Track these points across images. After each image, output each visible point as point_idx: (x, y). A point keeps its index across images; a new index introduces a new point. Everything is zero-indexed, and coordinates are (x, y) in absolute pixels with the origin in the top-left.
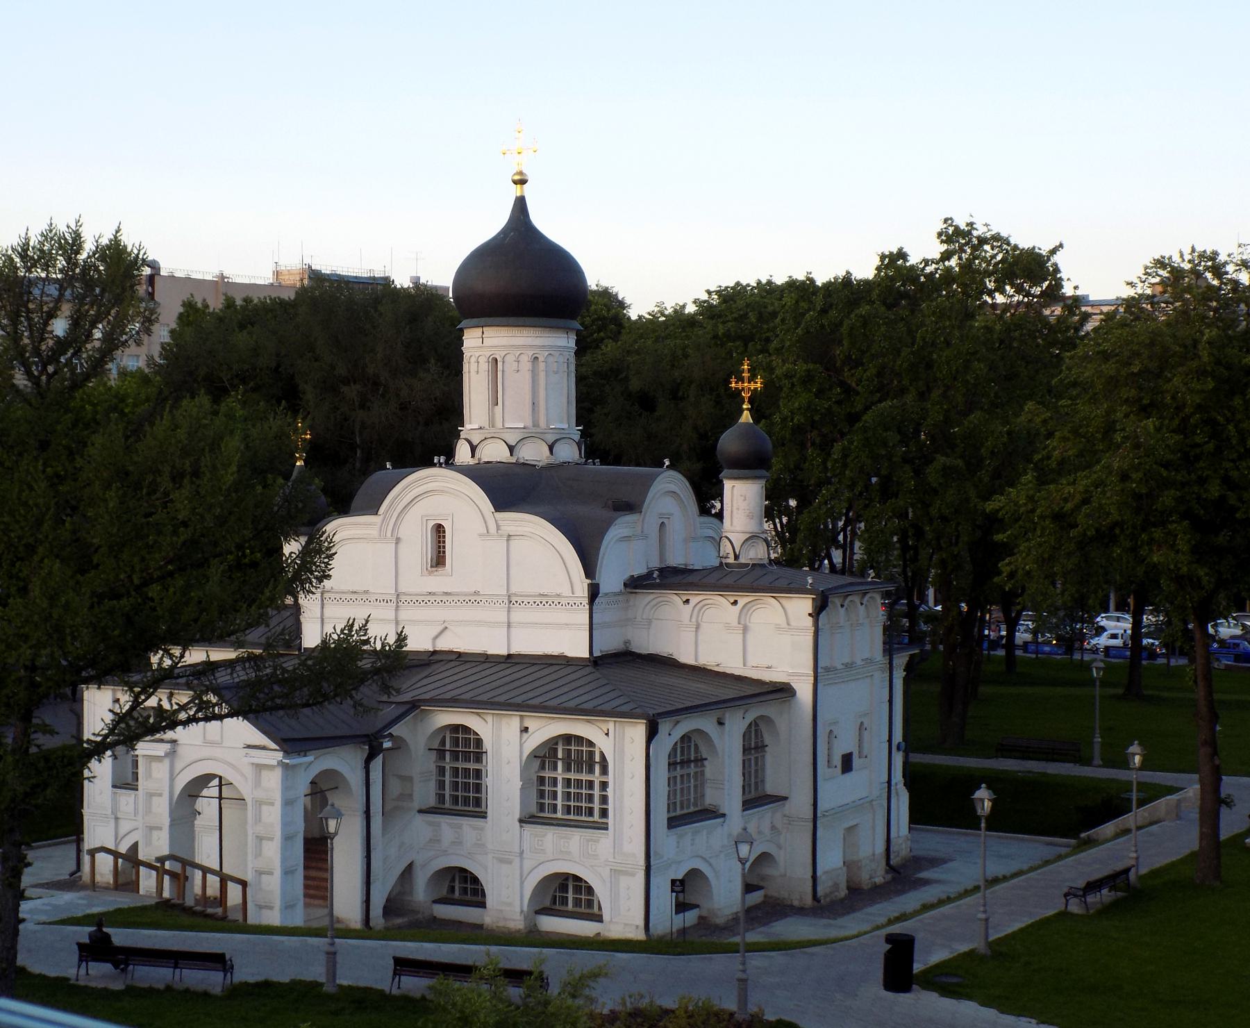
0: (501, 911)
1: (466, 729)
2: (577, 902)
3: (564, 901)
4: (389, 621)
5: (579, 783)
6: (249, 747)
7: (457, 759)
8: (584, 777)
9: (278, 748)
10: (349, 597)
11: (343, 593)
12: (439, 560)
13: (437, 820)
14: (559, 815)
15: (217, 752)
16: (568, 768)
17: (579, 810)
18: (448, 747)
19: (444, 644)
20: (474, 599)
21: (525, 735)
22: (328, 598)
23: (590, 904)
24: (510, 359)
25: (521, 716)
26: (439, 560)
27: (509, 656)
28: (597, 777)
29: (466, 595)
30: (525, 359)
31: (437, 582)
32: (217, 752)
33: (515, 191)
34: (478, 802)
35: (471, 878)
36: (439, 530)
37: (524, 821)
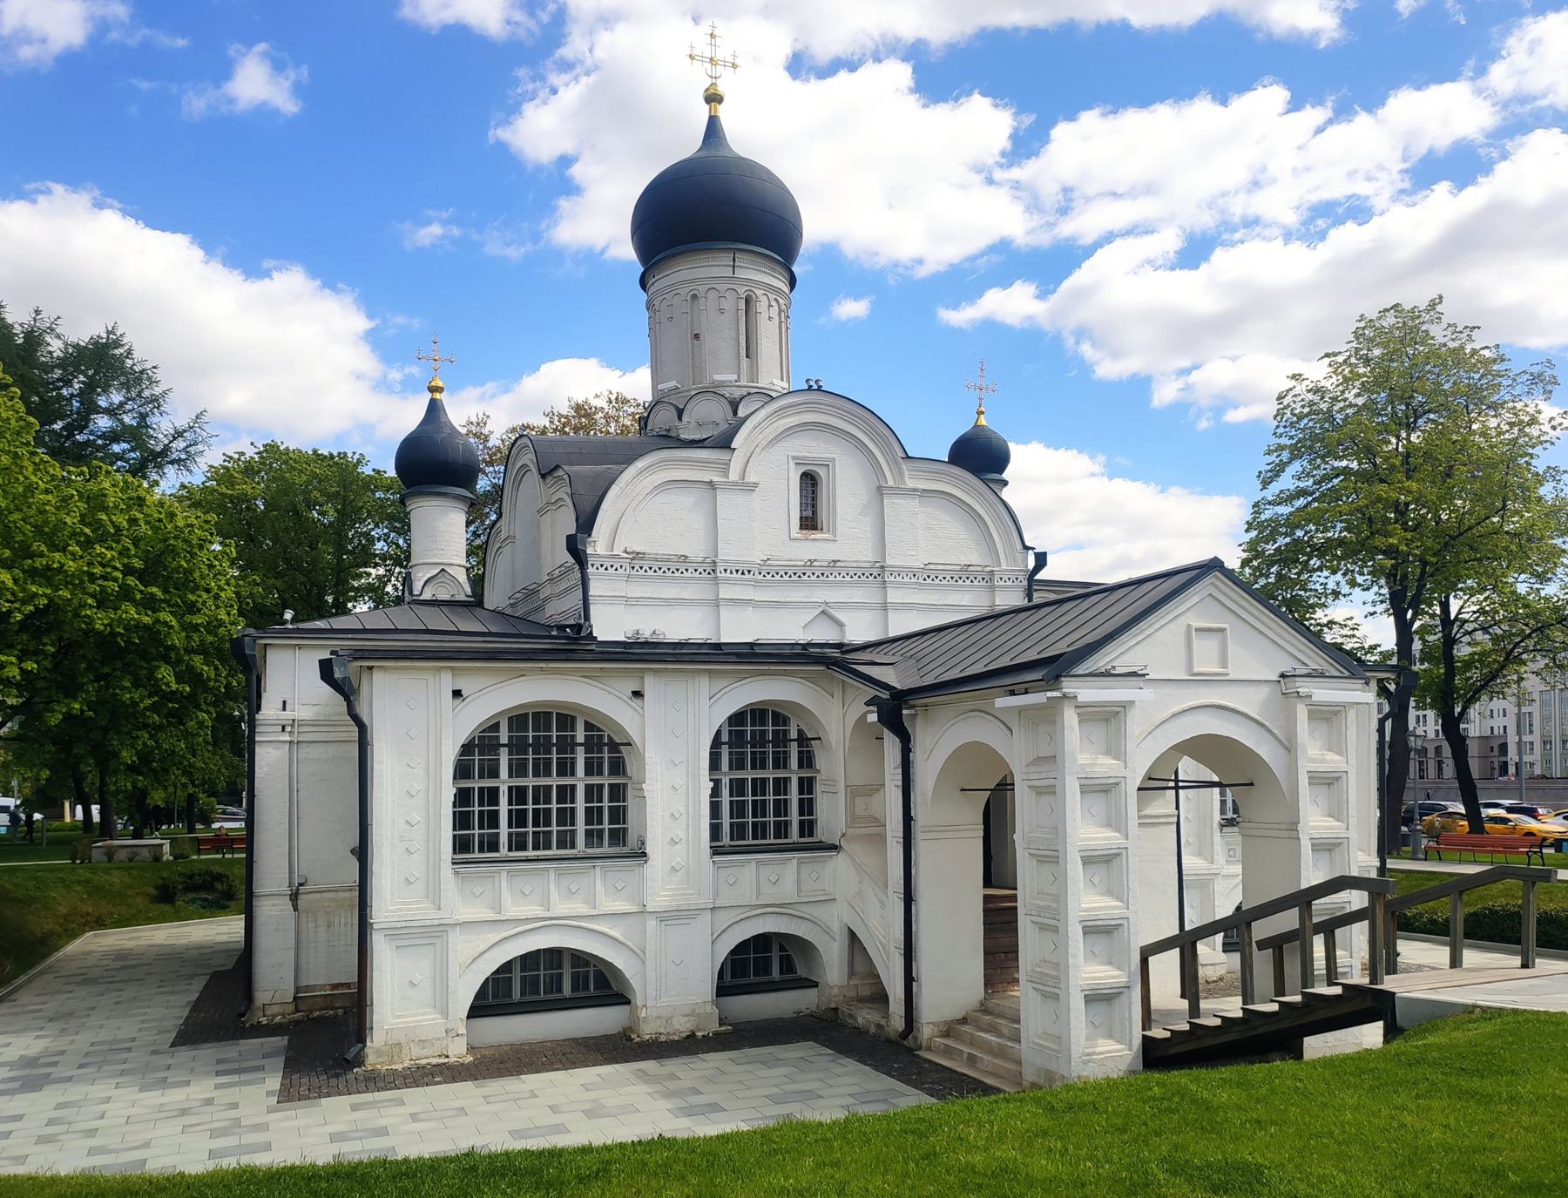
22: (637, 567)
26: (810, 522)
31: (814, 548)
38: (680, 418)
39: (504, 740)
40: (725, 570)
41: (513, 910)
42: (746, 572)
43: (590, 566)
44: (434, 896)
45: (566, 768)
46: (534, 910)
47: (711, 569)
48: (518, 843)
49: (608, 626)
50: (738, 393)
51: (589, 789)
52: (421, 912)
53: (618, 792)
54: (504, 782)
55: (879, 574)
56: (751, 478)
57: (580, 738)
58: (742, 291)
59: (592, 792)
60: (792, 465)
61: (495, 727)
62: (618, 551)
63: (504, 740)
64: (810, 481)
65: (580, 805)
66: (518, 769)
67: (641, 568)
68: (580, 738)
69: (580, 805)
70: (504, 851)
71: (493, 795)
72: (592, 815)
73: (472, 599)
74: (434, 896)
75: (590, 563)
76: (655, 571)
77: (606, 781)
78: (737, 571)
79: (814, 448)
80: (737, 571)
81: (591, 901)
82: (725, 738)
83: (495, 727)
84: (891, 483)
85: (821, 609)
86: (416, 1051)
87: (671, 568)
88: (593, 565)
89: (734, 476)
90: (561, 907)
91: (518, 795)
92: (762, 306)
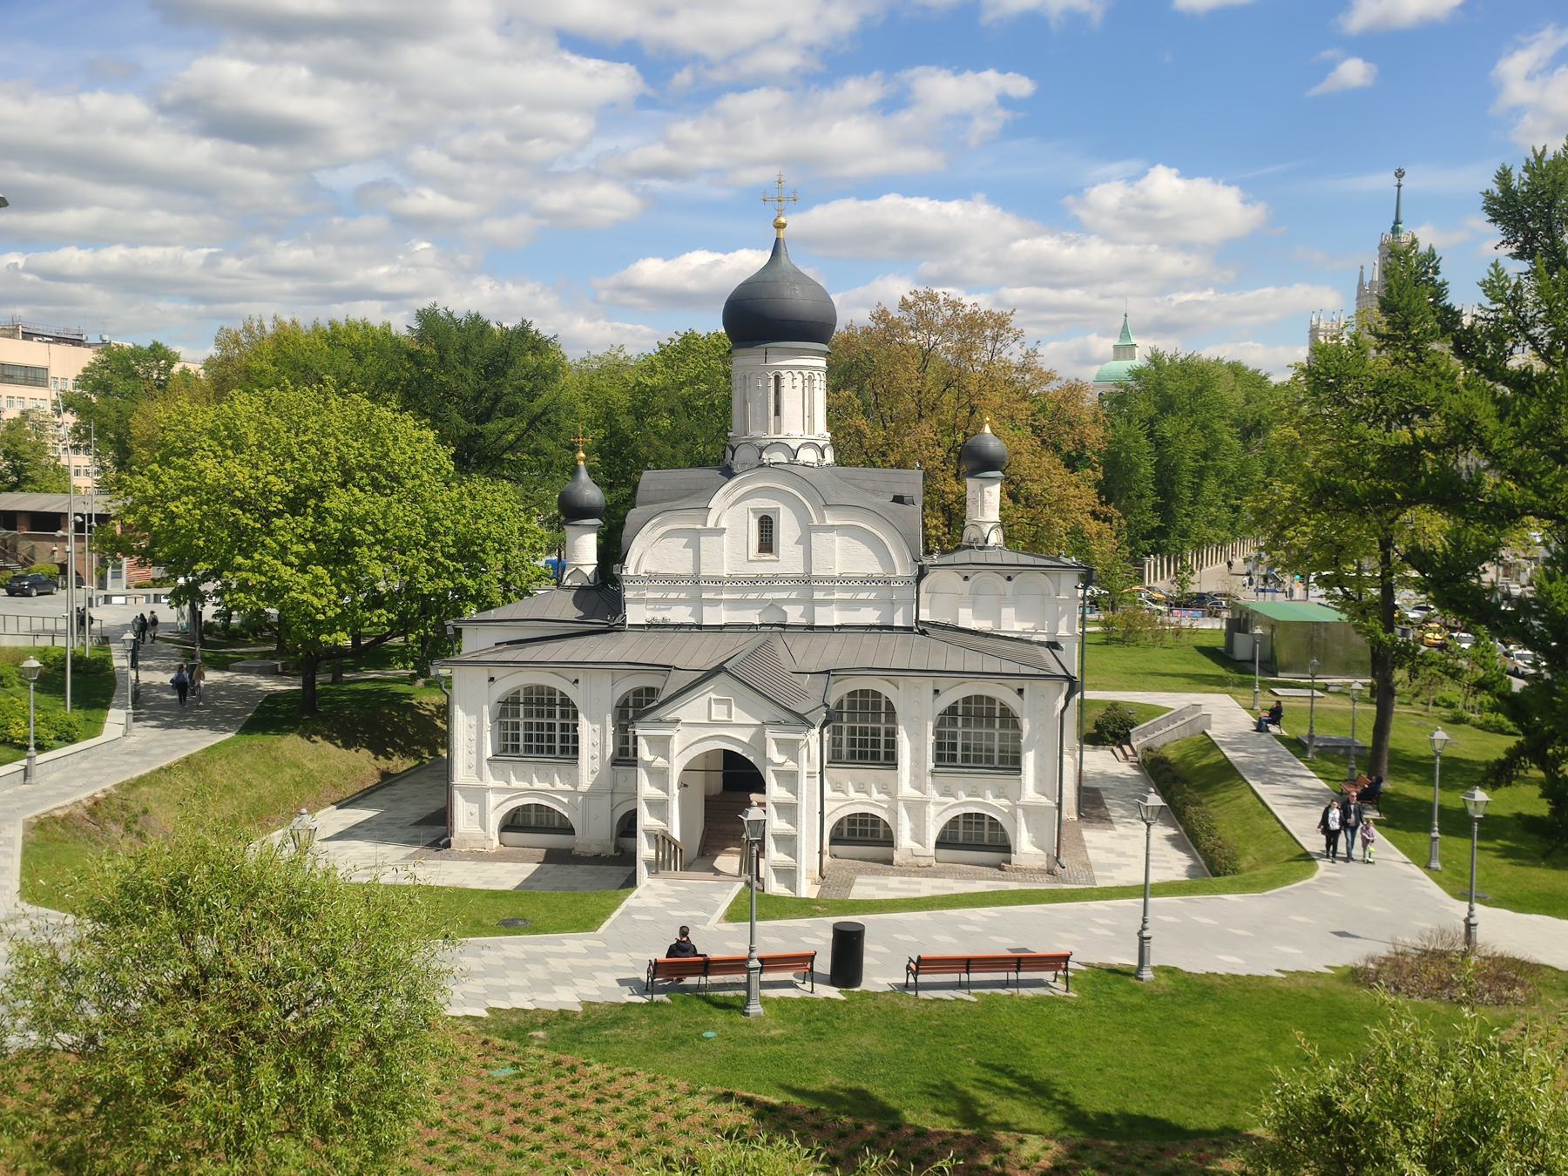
1: (877, 694)
12: (767, 543)
16: (966, 723)
18: (845, 709)
26: (767, 543)
33: (772, 234)
39: (522, 700)
41: (515, 783)
44: (480, 774)
45: (551, 714)
46: (525, 785)
47: (696, 580)
48: (529, 749)
50: (764, 443)
51: (562, 725)
52: (475, 781)
54: (522, 720)
55: (807, 581)
56: (723, 525)
57: (558, 701)
59: (564, 727)
60: (751, 514)
61: (518, 692)
62: (641, 572)
63: (522, 700)
65: (558, 733)
66: (528, 714)
68: (558, 701)
69: (558, 733)
71: (517, 726)
72: (564, 739)
74: (480, 774)
79: (766, 504)
81: (552, 784)
82: (631, 704)
83: (518, 692)
84: (816, 523)
86: (472, 844)
87: (672, 580)
89: (710, 524)
90: (537, 785)
91: (529, 726)
92: (786, 381)
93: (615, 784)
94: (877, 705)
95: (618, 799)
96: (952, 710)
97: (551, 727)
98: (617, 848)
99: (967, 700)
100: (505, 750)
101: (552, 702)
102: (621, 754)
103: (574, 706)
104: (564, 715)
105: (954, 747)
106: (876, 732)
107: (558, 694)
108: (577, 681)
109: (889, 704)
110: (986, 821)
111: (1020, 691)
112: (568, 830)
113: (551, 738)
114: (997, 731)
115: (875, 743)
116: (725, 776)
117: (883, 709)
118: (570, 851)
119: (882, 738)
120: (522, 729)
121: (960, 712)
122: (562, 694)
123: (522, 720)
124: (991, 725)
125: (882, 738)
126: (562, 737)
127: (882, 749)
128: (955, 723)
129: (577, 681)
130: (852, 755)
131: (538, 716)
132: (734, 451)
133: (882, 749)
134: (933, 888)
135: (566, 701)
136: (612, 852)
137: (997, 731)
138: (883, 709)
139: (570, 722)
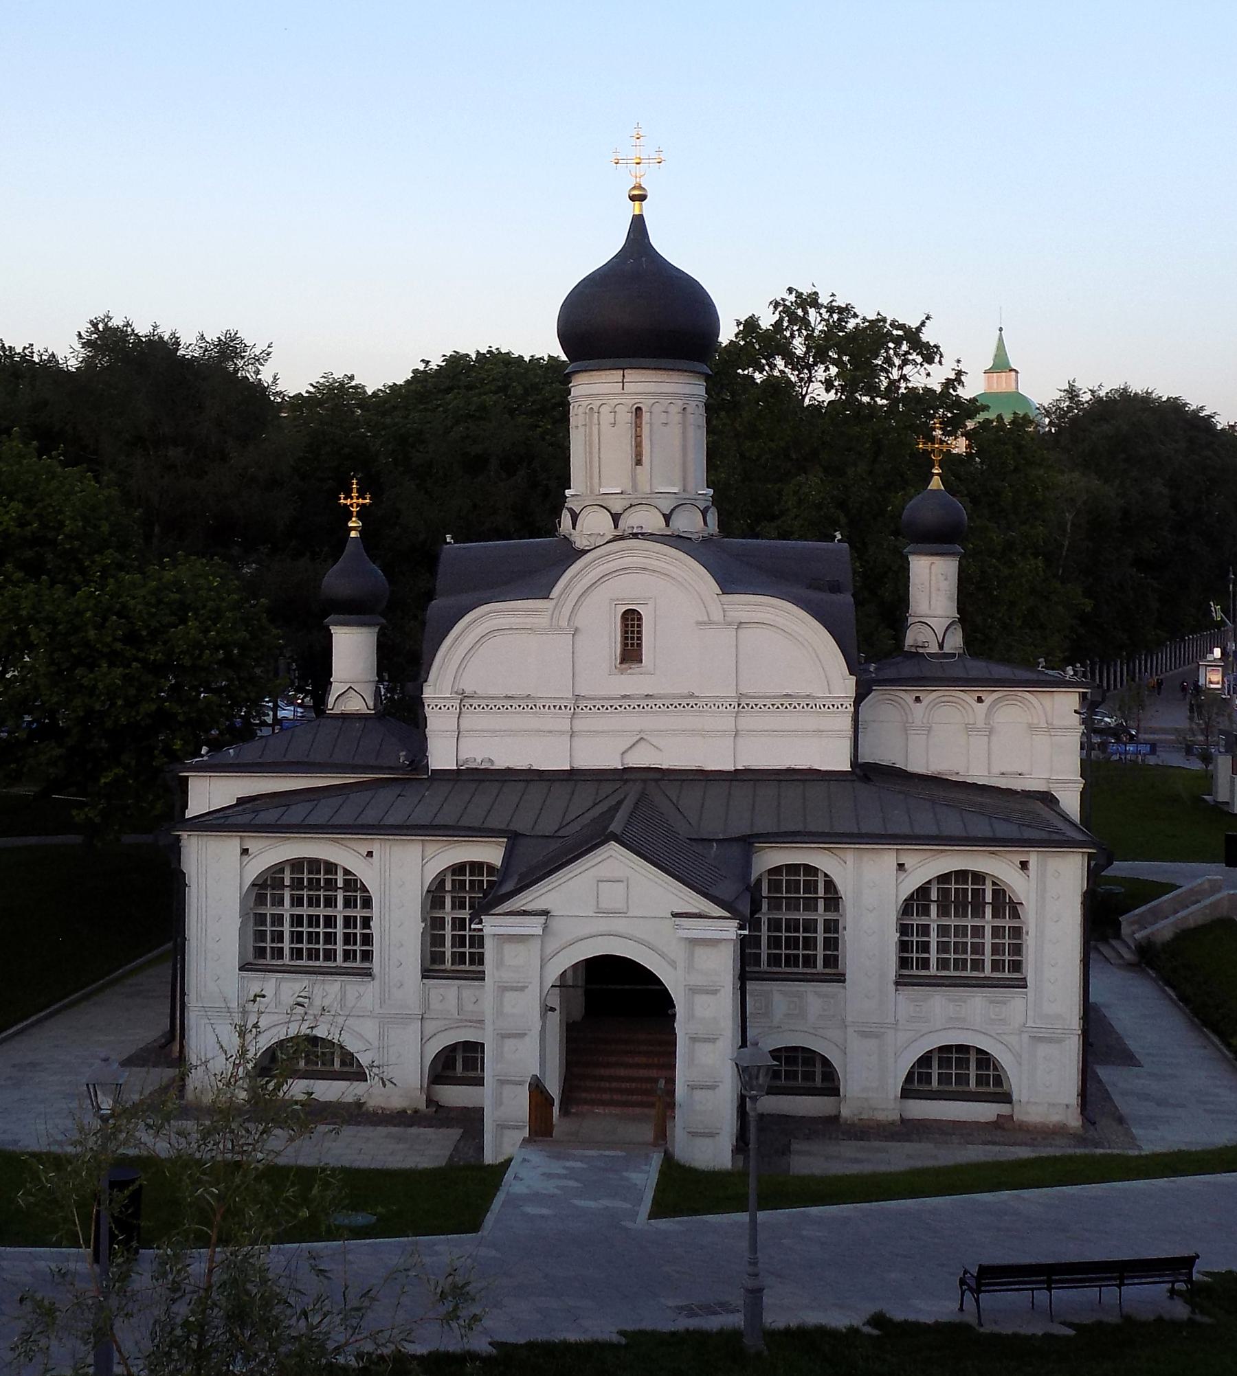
0: (866, 1099)
2: (981, 1080)
3: (963, 1079)
4: (562, 733)
5: (961, 931)
6: (675, 915)
7: (779, 908)
8: (969, 922)
9: (728, 915)
10: (616, 704)
11: (493, 698)
12: (631, 651)
13: (765, 988)
14: (933, 971)
15: (619, 925)
16: (943, 911)
17: (960, 964)
19: (641, 758)
20: (688, 702)
21: (903, 875)
22: (467, 705)
23: (998, 1081)
24: (658, 409)
25: (241, 837)
27: (572, 771)
28: (821, 915)
29: (675, 697)
30: (674, 410)
31: (633, 682)
32: (619, 925)
34: (1017, 966)
35: (920, 1067)
36: (631, 620)
37: (901, 982)
38: (574, 528)
39: (287, 882)
40: (544, 706)
42: (563, 707)
43: (426, 707)
45: (330, 902)
48: (297, 954)
49: (441, 756)
53: (367, 922)
57: (340, 884)
58: (631, 402)
59: (349, 922)
64: (631, 620)
65: (340, 930)
66: (297, 901)
67: (471, 706)
68: (340, 884)
69: (340, 930)
70: (286, 960)
71: (279, 919)
72: (348, 939)
73: (373, 712)
75: (426, 704)
76: (483, 708)
77: (358, 913)
78: (555, 706)
80: (555, 706)
82: (448, 887)
85: (638, 737)
88: (429, 705)
91: (297, 920)
93: (426, 1002)
94: (811, 887)
95: (430, 1027)
96: (923, 891)
97: (329, 921)
98: (430, 1102)
99: (943, 878)
100: (260, 952)
101: (331, 885)
102: (433, 961)
103: (364, 889)
104: (348, 903)
105: (925, 947)
106: (810, 926)
107: (340, 873)
108: (370, 854)
109: (830, 885)
110: (973, 1058)
111: (1024, 865)
112: (352, 1070)
113: (329, 938)
114: (988, 920)
115: (810, 943)
116: (589, 994)
117: (821, 893)
118: (359, 1105)
119: (820, 935)
120: (287, 923)
121: (934, 896)
122: (347, 872)
123: (287, 910)
124: (978, 912)
125: (820, 935)
126: (346, 936)
127: (820, 952)
128: (925, 911)
129: (370, 854)
130: (774, 960)
131: (310, 905)
132: (575, 517)
133: (820, 952)
134: (909, 1157)
135: (352, 883)
136: (422, 1106)
137: (988, 920)
138: (821, 893)
139: (358, 913)
